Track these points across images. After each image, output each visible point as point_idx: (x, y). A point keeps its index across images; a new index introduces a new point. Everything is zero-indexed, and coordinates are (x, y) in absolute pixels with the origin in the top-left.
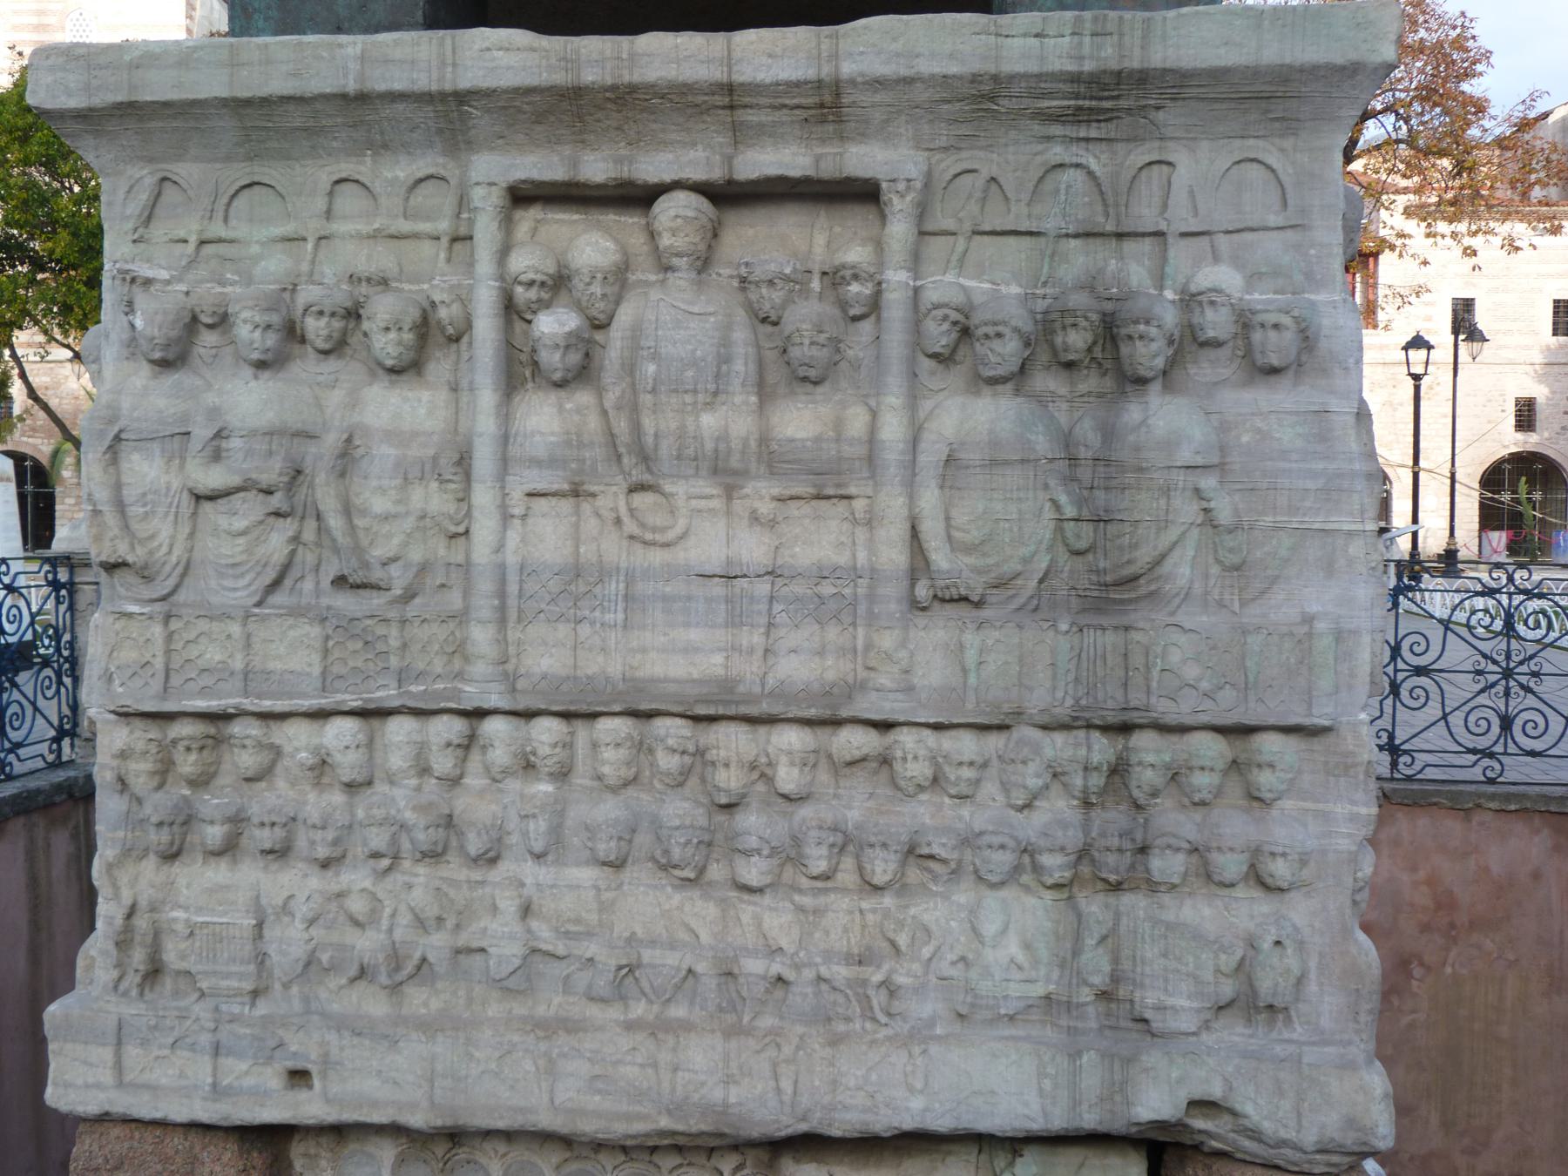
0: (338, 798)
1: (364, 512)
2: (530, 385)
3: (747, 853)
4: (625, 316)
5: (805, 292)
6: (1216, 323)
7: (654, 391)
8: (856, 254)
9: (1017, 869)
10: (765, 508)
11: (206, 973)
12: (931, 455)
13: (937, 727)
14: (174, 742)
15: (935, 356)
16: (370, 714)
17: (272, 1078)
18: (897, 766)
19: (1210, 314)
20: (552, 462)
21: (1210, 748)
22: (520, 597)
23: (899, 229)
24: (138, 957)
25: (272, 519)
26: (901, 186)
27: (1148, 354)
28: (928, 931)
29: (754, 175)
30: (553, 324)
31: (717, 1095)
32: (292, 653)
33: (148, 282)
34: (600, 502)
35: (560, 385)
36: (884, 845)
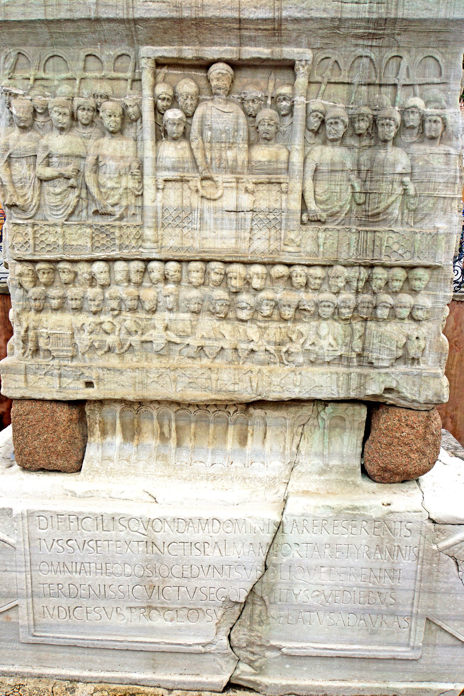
0: (98, 290)
1: (104, 186)
2: (164, 139)
3: (243, 309)
4: (199, 112)
5: (266, 104)
6: (414, 120)
7: (210, 142)
8: (286, 90)
9: (334, 314)
10: (251, 187)
11: (55, 350)
12: (310, 168)
13: (309, 266)
14: (39, 270)
15: (312, 131)
16: (109, 261)
17: (80, 385)
18: (294, 279)
19: (411, 116)
20: (174, 169)
21: (400, 274)
22: (162, 218)
24: (30, 345)
25: (69, 189)
26: (303, 63)
28: (302, 335)
29: (249, 57)
30: (173, 114)
31: (231, 388)
32: (80, 240)
33: (16, 95)
34: (191, 183)
35: (175, 139)
36: (289, 306)
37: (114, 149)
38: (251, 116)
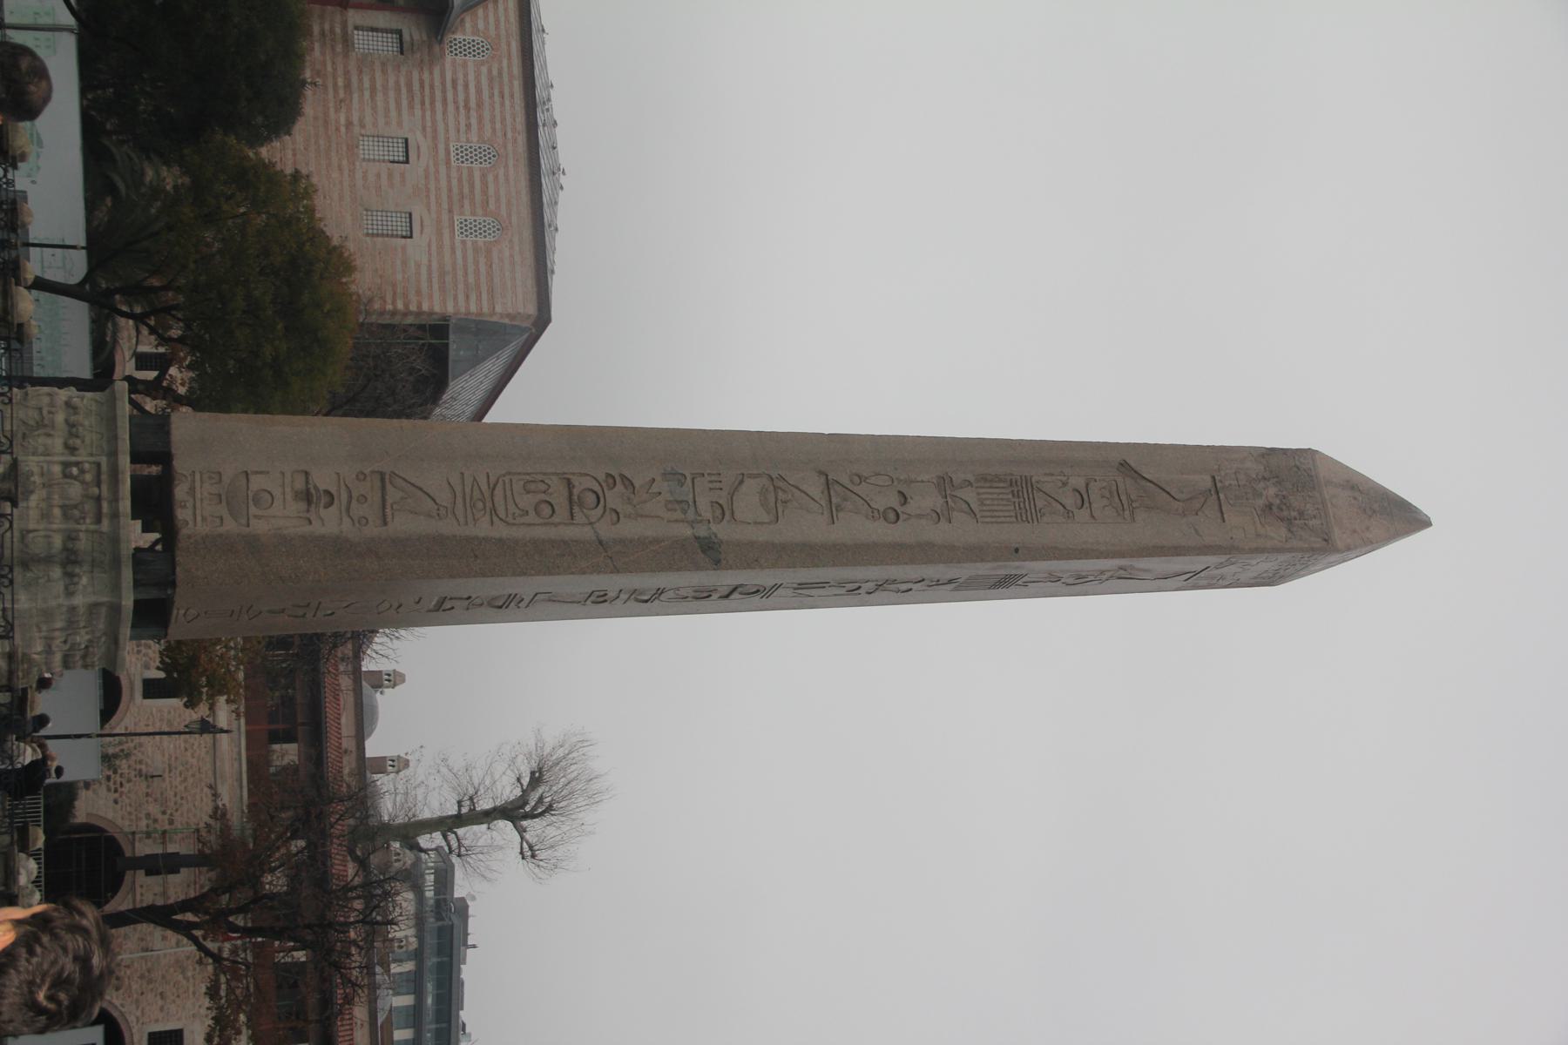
23: (93, 527)
27: (70, 568)
37: (58, 443)
38: (75, 507)
